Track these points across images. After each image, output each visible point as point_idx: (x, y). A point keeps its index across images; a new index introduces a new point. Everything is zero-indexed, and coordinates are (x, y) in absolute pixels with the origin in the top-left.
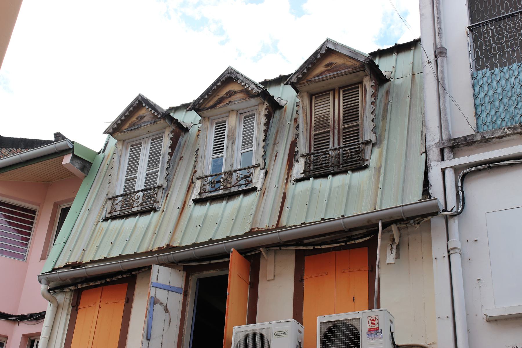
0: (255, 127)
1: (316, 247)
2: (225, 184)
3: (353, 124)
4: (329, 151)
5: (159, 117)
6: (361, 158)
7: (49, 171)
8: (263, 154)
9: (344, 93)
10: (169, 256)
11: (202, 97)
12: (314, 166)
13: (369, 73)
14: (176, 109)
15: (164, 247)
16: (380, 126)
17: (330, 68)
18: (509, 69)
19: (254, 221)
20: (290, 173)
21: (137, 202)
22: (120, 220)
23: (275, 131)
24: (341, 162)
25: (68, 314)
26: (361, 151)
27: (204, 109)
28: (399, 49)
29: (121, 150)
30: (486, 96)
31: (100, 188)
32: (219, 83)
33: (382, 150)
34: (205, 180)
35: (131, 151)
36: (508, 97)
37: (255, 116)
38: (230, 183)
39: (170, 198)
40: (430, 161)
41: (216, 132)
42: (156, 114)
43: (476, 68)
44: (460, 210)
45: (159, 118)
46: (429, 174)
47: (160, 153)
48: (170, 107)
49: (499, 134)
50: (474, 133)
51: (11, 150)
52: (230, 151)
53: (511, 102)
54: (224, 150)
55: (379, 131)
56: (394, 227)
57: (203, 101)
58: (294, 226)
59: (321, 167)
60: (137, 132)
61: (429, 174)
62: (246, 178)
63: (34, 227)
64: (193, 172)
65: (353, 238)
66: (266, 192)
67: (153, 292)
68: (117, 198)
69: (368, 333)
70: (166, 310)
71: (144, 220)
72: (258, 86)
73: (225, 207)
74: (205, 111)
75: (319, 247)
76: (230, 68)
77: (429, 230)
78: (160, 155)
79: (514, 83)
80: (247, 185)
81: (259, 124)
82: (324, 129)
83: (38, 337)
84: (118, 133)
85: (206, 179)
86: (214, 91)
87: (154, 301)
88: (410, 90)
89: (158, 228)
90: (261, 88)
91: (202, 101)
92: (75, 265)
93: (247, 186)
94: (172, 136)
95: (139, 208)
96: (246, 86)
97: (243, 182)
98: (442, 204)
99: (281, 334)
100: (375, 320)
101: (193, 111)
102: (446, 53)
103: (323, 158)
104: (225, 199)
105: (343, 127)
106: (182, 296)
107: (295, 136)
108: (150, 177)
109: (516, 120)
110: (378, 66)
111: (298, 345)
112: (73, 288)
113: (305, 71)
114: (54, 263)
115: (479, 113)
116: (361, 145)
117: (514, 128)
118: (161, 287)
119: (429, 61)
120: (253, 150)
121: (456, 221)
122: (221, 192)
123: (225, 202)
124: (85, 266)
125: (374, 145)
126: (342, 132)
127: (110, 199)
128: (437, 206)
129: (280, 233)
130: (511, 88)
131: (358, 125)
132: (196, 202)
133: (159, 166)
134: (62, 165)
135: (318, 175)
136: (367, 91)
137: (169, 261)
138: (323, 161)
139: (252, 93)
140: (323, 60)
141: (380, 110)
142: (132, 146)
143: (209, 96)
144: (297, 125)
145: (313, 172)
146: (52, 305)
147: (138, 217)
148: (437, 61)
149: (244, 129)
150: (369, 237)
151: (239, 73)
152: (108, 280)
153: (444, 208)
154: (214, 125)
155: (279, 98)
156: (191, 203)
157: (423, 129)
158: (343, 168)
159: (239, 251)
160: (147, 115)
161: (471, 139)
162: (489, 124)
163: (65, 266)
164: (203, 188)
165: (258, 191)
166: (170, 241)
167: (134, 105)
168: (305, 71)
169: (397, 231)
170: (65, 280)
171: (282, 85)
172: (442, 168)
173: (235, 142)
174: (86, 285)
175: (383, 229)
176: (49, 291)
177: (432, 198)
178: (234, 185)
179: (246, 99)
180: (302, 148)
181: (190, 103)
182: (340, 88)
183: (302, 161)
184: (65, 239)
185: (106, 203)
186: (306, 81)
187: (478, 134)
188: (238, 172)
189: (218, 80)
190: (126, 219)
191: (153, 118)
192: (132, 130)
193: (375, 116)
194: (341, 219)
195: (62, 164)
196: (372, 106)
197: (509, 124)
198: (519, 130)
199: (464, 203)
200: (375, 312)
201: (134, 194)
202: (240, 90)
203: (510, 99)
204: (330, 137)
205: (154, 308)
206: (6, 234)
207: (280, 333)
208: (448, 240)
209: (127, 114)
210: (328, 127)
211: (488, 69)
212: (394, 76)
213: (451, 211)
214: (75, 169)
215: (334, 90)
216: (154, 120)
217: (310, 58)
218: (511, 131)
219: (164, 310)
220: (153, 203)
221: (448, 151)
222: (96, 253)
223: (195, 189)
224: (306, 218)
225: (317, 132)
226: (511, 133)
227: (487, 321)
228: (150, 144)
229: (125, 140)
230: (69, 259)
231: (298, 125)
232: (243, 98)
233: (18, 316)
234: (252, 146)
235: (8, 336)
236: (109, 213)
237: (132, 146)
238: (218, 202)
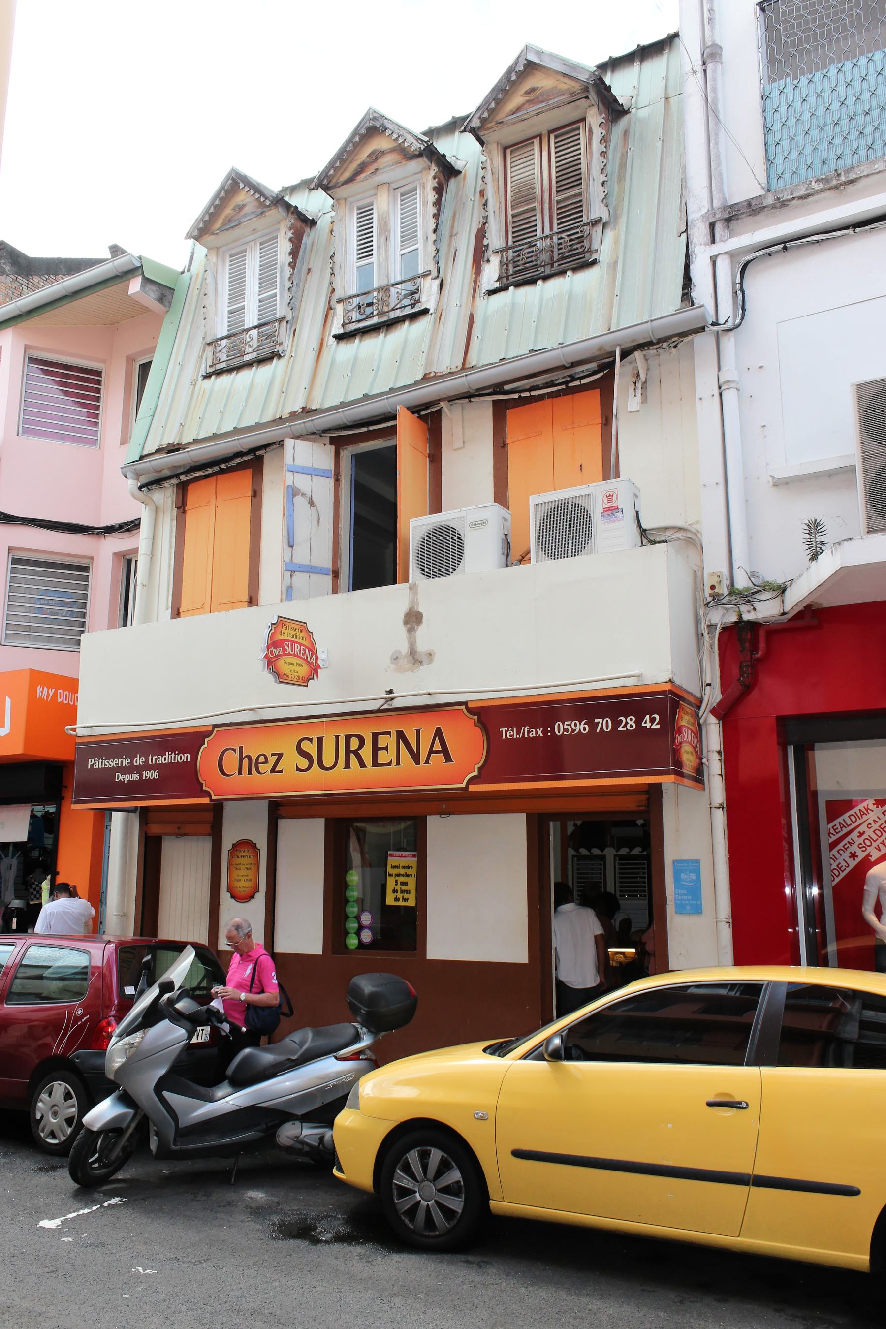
0: (418, 210)
1: (523, 395)
2: (379, 307)
3: (573, 193)
4: (537, 240)
5: (267, 204)
6: (586, 249)
7: (110, 306)
8: (434, 253)
9: (556, 141)
10: (308, 425)
11: (331, 165)
12: (514, 267)
13: (596, 100)
14: (293, 189)
15: (298, 411)
16: (615, 193)
17: (532, 96)
18: (823, 76)
19: (429, 362)
20: (478, 281)
21: (250, 346)
22: (229, 375)
23: (451, 214)
24: (556, 257)
25: (172, 520)
26: (586, 237)
27: (335, 187)
28: (645, 53)
29: (216, 264)
30: (784, 126)
31: (191, 327)
32: (357, 139)
33: (618, 232)
34: (350, 302)
35: (230, 266)
36: (819, 127)
37: (418, 191)
38: (388, 305)
39: (299, 335)
40: (693, 245)
41: (358, 218)
42: (262, 199)
43: (769, 77)
44: (738, 321)
45: (269, 206)
46: (691, 267)
47: (276, 264)
48: (283, 187)
49: (802, 192)
50: (762, 192)
51: (47, 279)
52: (384, 252)
53: (824, 134)
54: (374, 252)
55: (613, 201)
56: (637, 355)
57: (335, 171)
58: (488, 365)
59: (525, 269)
60: (237, 232)
61: (692, 267)
62: (412, 294)
63: (102, 395)
64: (330, 291)
65: (577, 376)
66: (444, 314)
67: (289, 478)
68: (219, 342)
69: (603, 514)
70: (312, 503)
71: (264, 372)
72: (419, 139)
73: (383, 344)
74: (339, 189)
75: (527, 394)
76: (371, 111)
77: (691, 357)
78: (276, 268)
79: (830, 100)
80: (413, 305)
81: (425, 204)
82: (527, 204)
83: (136, 555)
84: (207, 235)
85: (351, 300)
86: (350, 153)
87: (293, 492)
88: (662, 126)
89: (286, 382)
90: (424, 141)
91: (331, 172)
92: (173, 449)
93: (414, 307)
94: (292, 236)
95: (255, 355)
96: (400, 140)
97: (407, 302)
98: (711, 313)
99: (478, 524)
100: (613, 496)
101: (320, 189)
102: (721, 55)
103: (528, 253)
104: (382, 331)
105: (556, 199)
106: (331, 482)
107: (482, 220)
108: (265, 304)
109: (829, 166)
110: (610, 87)
111: (504, 537)
112: (174, 481)
113: (493, 105)
114: (141, 447)
115: (771, 159)
116: (585, 227)
117: (826, 180)
118: (299, 471)
119: (694, 70)
120: (418, 249)
121: (732, 339)
122: (375, 320)
123: (382, 335)
124: (186, 448)
125: (605, 226)
126: (555, 207)
127: (209, 344)
128: (703, 317)
129: (468, 377)
130: (825, 109)
131: (580, 194)
132: (339, 338)
133: (276, 285)
134: (129, 296)
135: (520, 282)
136: (592, 133)
137: (307, 432)
138: (527, 258)
139: (410, 152)
140: (521, 83)
141: (613, 167)
142: (231, 256)
143: (343, 161)
144: (484, 202)
145: (514, 278)
146: (147, 508)
147: (254, 368)
148: (705, 71)
149: (402, 214)
150: (602, 374)
151: (386, 118)
152: (223, 466)
153: (714, 320)
154: (355, 212)
155: (454, 158)
156: (332, 341)
157: (682, 193)
158: (559, 267)
159: (408, 408)
160: (249, 202)
161: (757, 203)
162: (787, 176)
163: (158, 451)
164: (348, 315)
165: (431, 314)
166: (307, 402)
167: (226, 187)
168: (493, 105)
169: (644, 361)
170: (161, 471)
171: (457, 133)
172: (712, 255)
173: (390, 237)
174: (191, 476)
175: (622, 359)
176: (140, 488)
177: (696, 305)
178: (394, 307)
179: (401, 163)
180: (495, 239)
181: (313, 179)
182: (550, 132)
183: (495, 260)
184: (152, 410)
185: (204, 351)
186: (495, 123)
187: (770, 194)
188: (399, 286)
189: (355, 133)
190: (237, 373)
191: (258, 208)
192: (228, 229)
193: (606, 176)
194: (558, 348)
195: (130, 293)
196: (602, 159)
197: (818, 173)
198: (834, 183)
199: (744, 309)
200: (612, 484)
201: (245, 333)
202: (391, 149)
203: (822, 129)
204: (537, 217)
205: (294, 502)
206: (64, 410)
207: (477, 523)
208: (719, 369)
209: (217, 202)
210: (533, 200)
211: (789, 78)
212: (636, 103)
213: (724, 324)
214: (150, 299)
215: (540, 136)
216: (260, 211)
217: (499, 81)
218: (821, 186)
219: (309, 503)
220: (275, 346)
221: (722, 227)
222: (200, 427)
223: (335, 318)
224: (506, 351)
225: (516, 211)
226: (821, 189)
227: (774, 486)
228: (258, 251)
229: (220, 247)
230: (162, 439)
231: (487, 200)
232: (396, 161)
233: (102, 528)
234: (416, 242)
235: (93, 557)
236: (210, 366)
237: (231, 256)
238: (372, 336)
